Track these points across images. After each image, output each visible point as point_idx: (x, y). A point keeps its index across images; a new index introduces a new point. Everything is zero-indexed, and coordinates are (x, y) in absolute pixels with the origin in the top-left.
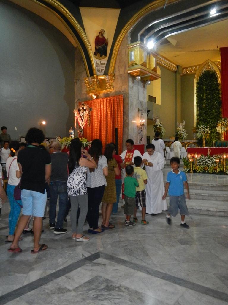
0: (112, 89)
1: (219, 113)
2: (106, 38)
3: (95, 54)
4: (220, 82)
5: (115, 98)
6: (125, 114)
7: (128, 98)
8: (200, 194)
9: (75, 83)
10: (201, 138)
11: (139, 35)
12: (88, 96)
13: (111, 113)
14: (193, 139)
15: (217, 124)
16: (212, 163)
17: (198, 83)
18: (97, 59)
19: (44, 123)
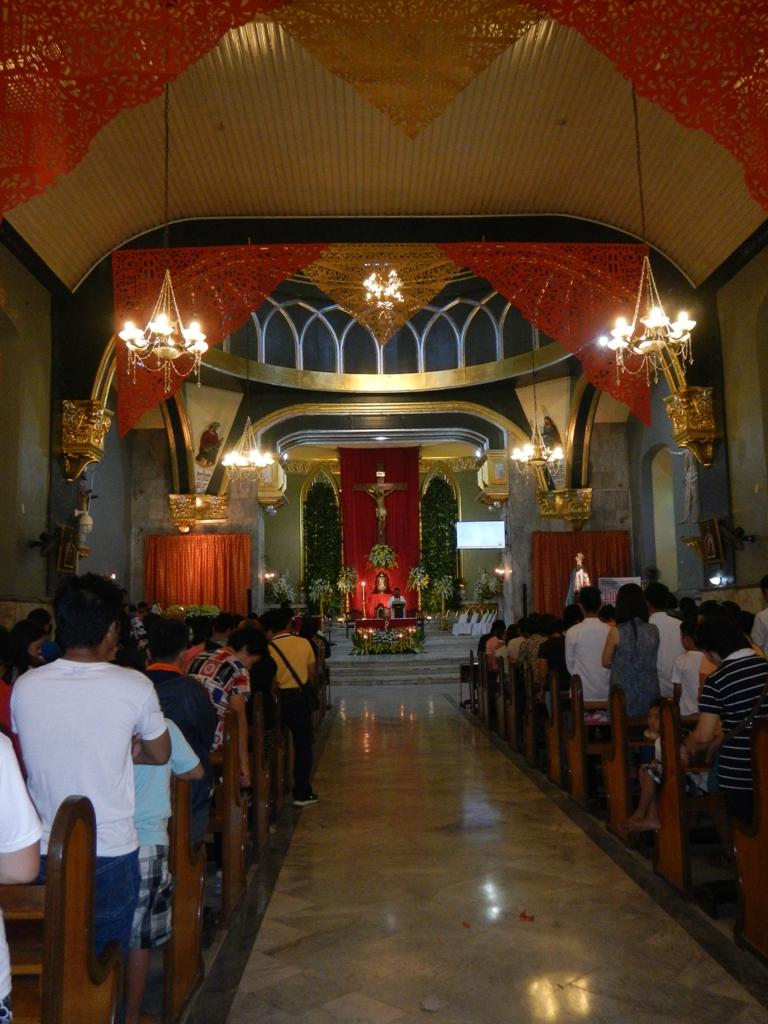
0: (222, 521)
1: (337, 558)
2: (219, 438)
3: (198, 459)
4: (338, 504)
5: (233, 538)
6: (254, 565)
7: (257, 539)
8: (428, 669)
9: (132, 497)
10: (318, 602)
11: (278, 443)
12: (166, 525)
13: (225, 560)
14: (300, 603)
15: (337, 577)
16: (393, 640)
17: (305, 503)
18: (201, 466)
19: (114, 576)
